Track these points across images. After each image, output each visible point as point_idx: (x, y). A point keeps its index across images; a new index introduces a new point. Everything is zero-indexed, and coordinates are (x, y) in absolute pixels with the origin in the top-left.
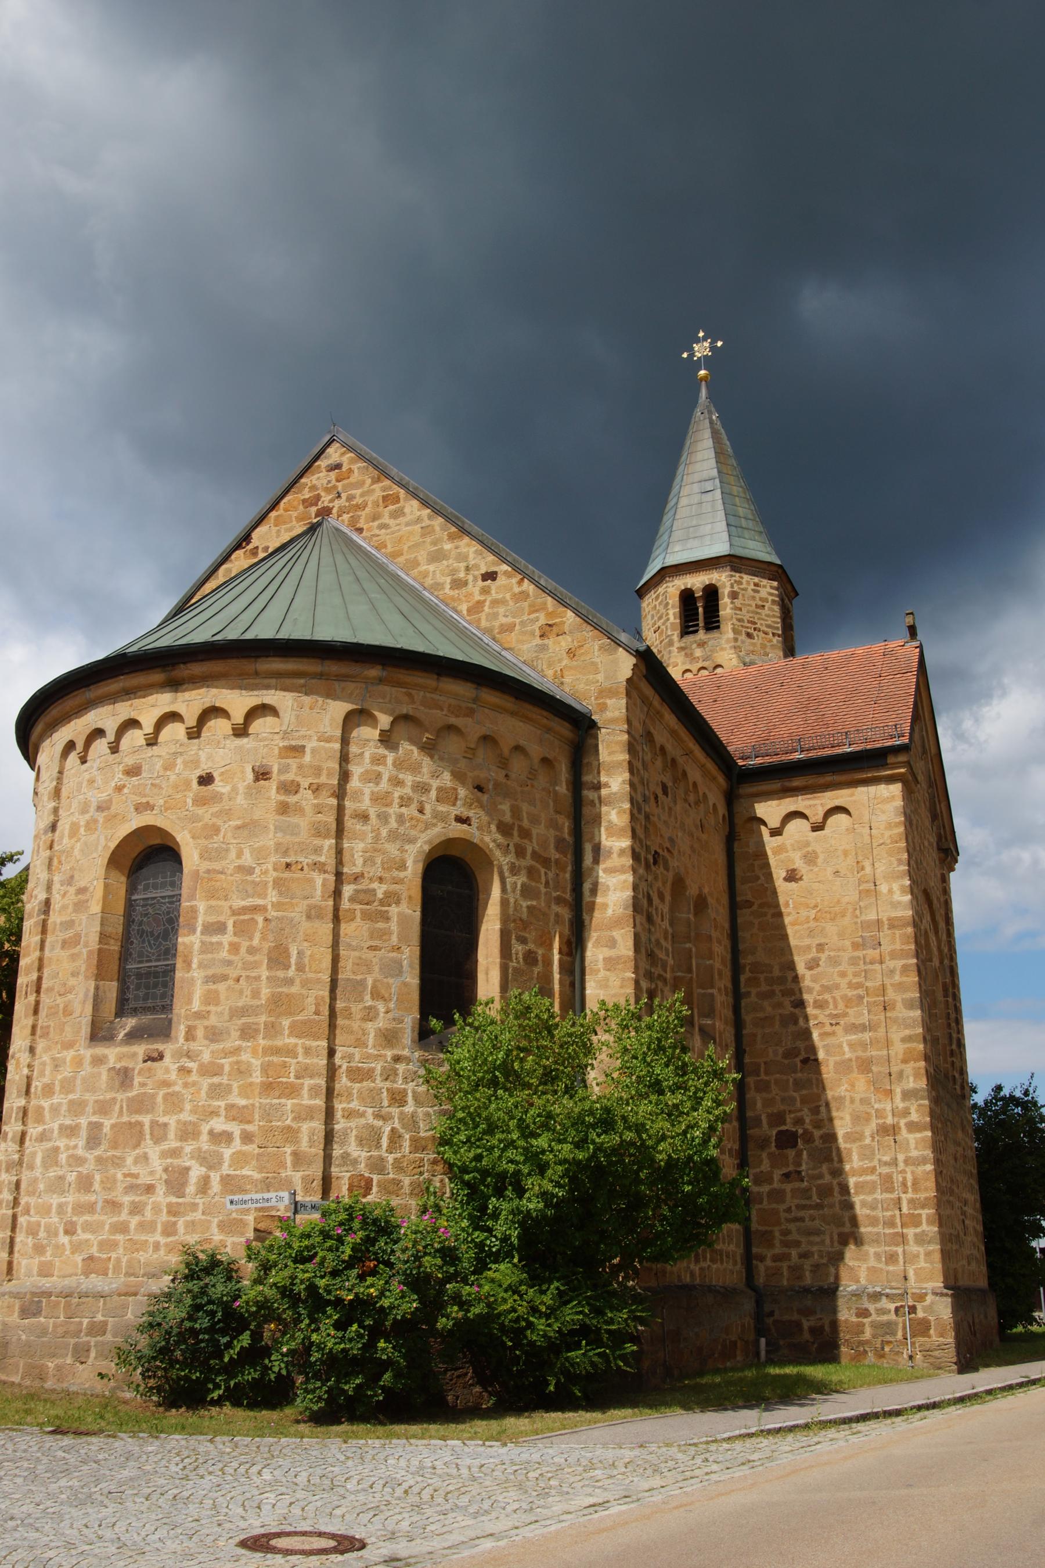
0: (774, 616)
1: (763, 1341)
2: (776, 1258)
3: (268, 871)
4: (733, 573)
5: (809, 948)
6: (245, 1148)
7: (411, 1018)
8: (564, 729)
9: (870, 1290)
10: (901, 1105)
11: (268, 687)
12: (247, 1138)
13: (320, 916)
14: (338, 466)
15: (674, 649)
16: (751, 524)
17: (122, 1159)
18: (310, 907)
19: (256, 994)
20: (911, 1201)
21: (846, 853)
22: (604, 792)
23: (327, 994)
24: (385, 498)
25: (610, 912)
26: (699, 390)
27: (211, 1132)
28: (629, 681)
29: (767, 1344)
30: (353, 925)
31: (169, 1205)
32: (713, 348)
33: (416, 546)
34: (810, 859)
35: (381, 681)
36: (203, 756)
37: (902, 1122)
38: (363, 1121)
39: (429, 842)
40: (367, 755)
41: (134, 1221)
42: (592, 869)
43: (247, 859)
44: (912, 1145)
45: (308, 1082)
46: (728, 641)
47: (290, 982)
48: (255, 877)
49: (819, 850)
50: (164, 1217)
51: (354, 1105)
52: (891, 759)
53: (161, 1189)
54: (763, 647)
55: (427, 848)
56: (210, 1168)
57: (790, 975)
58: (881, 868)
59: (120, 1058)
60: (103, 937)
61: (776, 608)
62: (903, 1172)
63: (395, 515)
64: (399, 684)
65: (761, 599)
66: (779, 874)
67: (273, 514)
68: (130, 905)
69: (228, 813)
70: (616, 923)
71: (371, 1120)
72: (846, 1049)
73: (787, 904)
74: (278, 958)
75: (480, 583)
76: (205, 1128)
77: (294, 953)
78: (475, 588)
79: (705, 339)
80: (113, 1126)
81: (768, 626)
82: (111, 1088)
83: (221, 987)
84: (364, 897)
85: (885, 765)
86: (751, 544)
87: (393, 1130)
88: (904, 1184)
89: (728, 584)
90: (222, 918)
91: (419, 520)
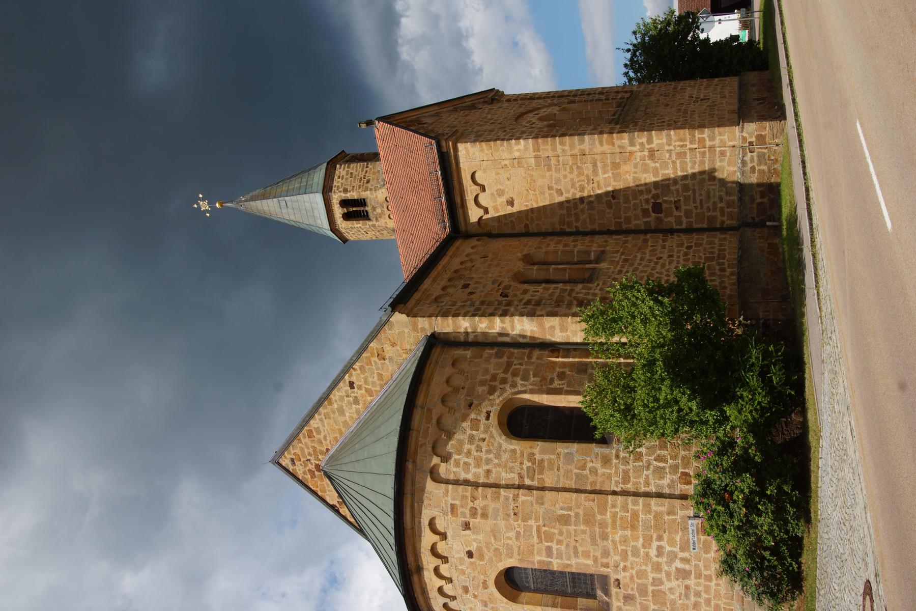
1: (768, 223)
2: (723, 215)
3: (519, 525)
5: (550, 194)
6: (665, 539)
7: (596, 449)
8: (436, 352)
9: (740, 165)
10: (638, 147)
11: (420, 523)
12: (660, 538)
13: (542, 498)
14: (292, 460)
15: (377, 224)
16: (304, 180)
17: (672, 600)
18: (537, 503)
19: (584, 532)
20: (691, 143)
21: (497, 174)
22: (469, 330)
23: (583, 495)
24: (309, 437)
25: (535, 329)
26: (228, 207)
27: (657, 556)
28: (408, 316)
29: (770, 221)
30: (546, 479)
31: (696, 578)
32: (203, 199)
33: (335, 422)
34: (501, 193)
35: (414, 462)
36: (457, 556)
37: (647, 146)
38: (651, 476)
39: (500, 435)
40: (455, 470)
41: (704, 595)
42: (512, 338)
43: (512, 534)
44: (660, 141)
45: (630, 506)
46: (372, 194)
47: (577, 514)
48: (522, 531)
49: (496, 188)
50: (702, 581)
51: (642, 481)
52: (444, 150)
53: (687, 582)
54: (374, 173)
55: (504, 437)
56: (676, 557)
57: (566, 205)
58: (506, 155)
59: (619, 600)
60: (554, 605)
61: (352, 165)
62: (675, 146)
63: (319, 432)
64: (416, 452)
66: (509, 210)
67: (319, 493)
68: (537, 591)
69: (488, 544)
70: (541, 325)
71: (650, 472)
72: (606, 175)
73: (526, 206)
74: (564, 520)
75: (355, 390)
76: (655, 559)
77: (562, 512)
78: (358, 393)
79: (198, 204)
80: (654, 604)
82: (634, 605)
83: (580, 549)
84: (531, 473)
85: (448, 153)
86: (316, 180)
87: (655, 460)
88: (682, 146)
90: (544, 548)
91: (321, 420)
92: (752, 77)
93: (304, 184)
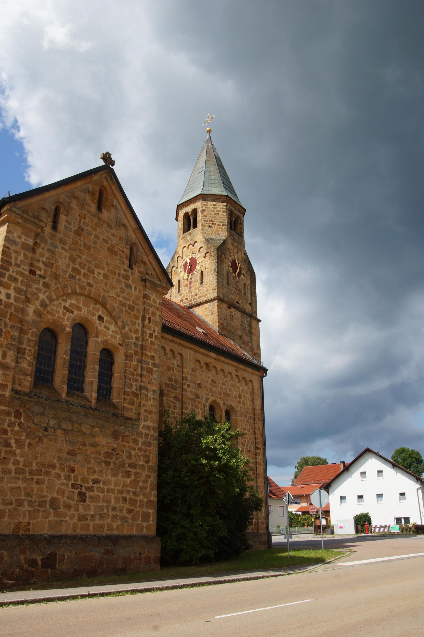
0: (223, 217)
4: (203, 202)
15: (181, 239)
46: (199, 231)
54: (217, 231)
61: (225, 214)
65: (217, 211)
86: (214, 189)
89: (201, 207)
92: (154, 551)
93: (213, 181)
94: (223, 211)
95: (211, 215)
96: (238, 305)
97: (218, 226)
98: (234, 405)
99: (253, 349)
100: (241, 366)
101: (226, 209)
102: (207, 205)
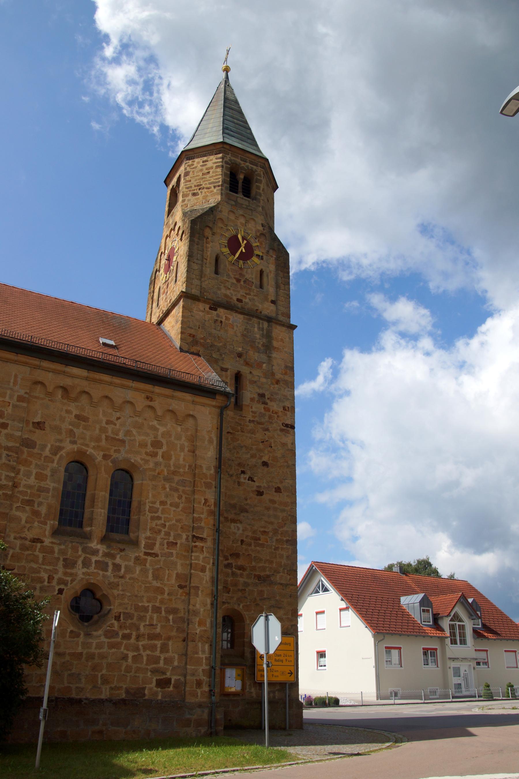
0: (217, 175)
61: (219, 170)
81: (210, 184)
94: (217, 167)
95: (198, 178)
96: (239, 305)
97: (206, 190)
98: (136, 459)
99: (273, 374)
100: (158, 389)
101: (222, 162)
102: (193, 165)
